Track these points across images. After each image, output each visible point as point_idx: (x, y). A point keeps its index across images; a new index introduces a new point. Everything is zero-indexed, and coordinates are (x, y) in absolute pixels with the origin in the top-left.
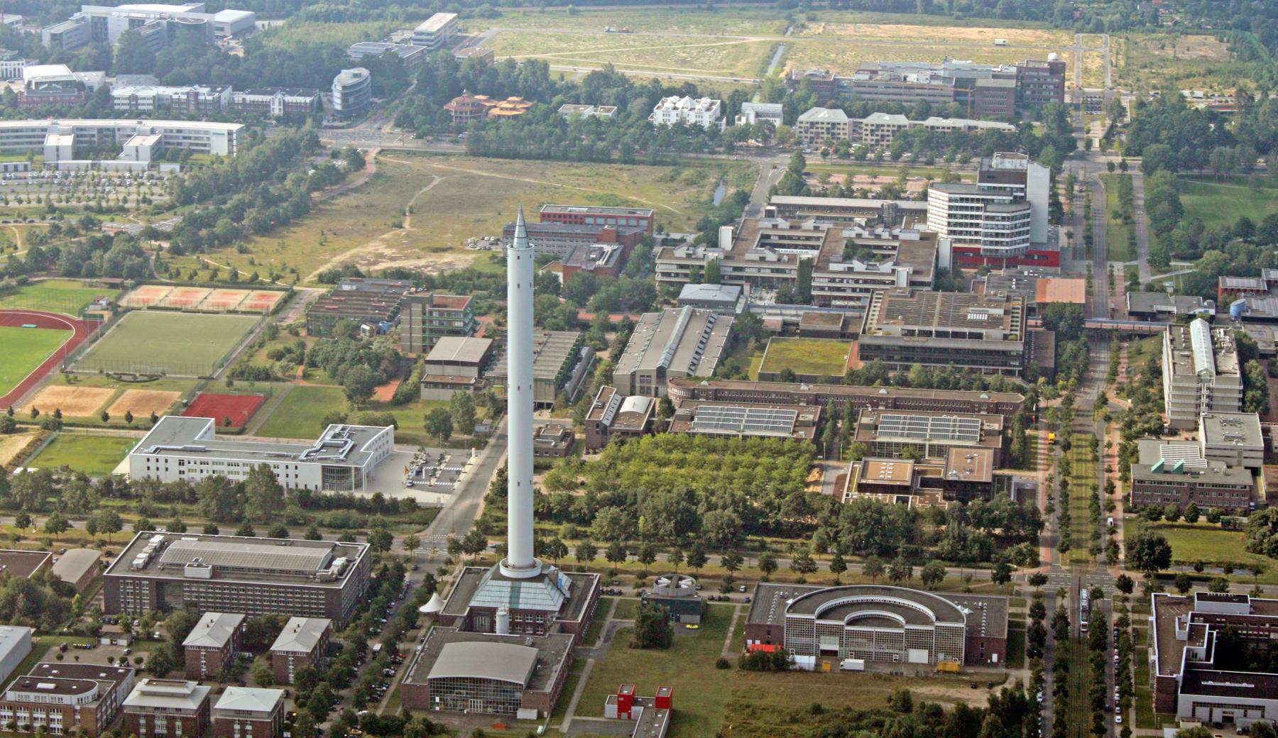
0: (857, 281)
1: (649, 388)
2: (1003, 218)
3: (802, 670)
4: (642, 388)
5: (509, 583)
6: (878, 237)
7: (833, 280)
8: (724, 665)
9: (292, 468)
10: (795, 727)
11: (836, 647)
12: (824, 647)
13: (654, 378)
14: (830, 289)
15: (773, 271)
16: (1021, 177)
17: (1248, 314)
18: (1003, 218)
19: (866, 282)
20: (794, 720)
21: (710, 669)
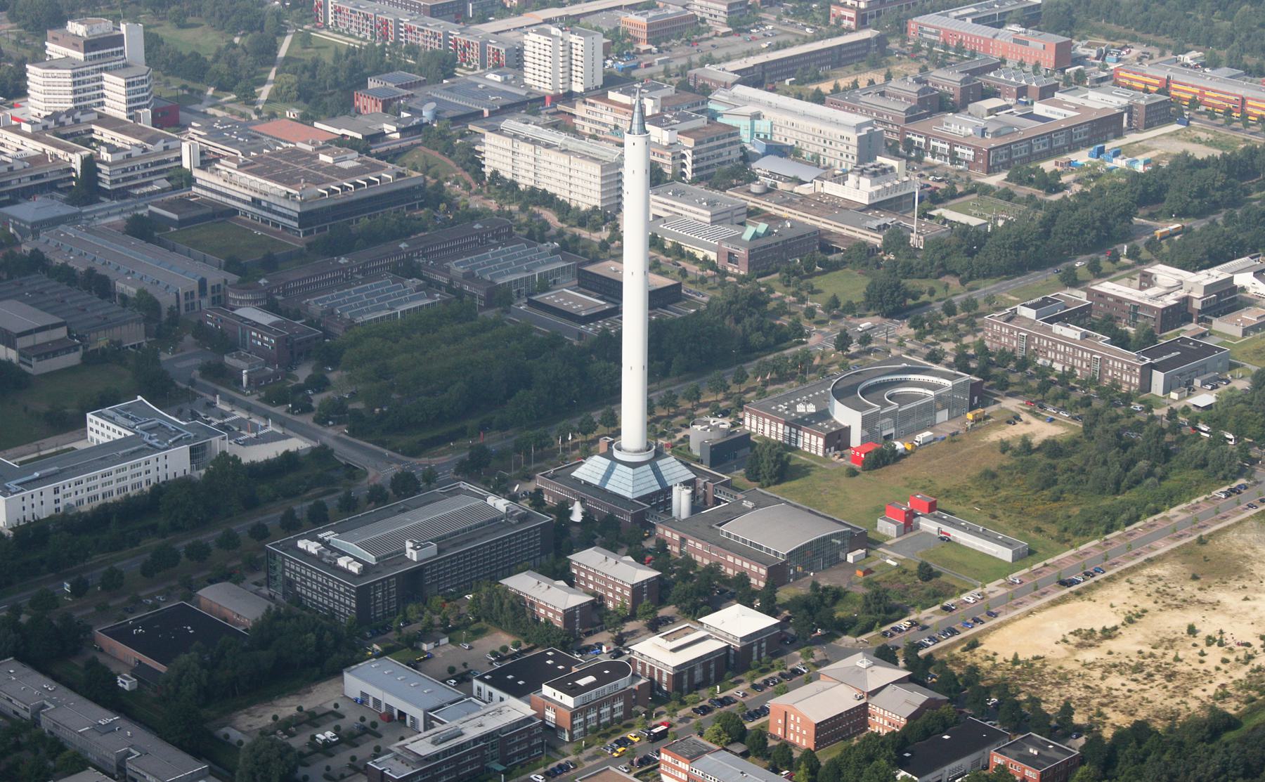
0: (146, 166)
1: (193, 304)
2: (142, 82)
3: (904, 455)
4: (187, 306)
5: (648, 467)
6: (62, 124)
7: (126, 171)
8: (853, 473)
9: (162, 459)
10: (1003, 493)
11: (893, 431)
12: (885, 433)
13: (197, 294)
14: (125, 180)
15: (32, 178)
16: (118, 40)
17: (450, 114)
18: (142, 82)
19: (153, 164)
20: (997, 488)
21: (846, 483)
